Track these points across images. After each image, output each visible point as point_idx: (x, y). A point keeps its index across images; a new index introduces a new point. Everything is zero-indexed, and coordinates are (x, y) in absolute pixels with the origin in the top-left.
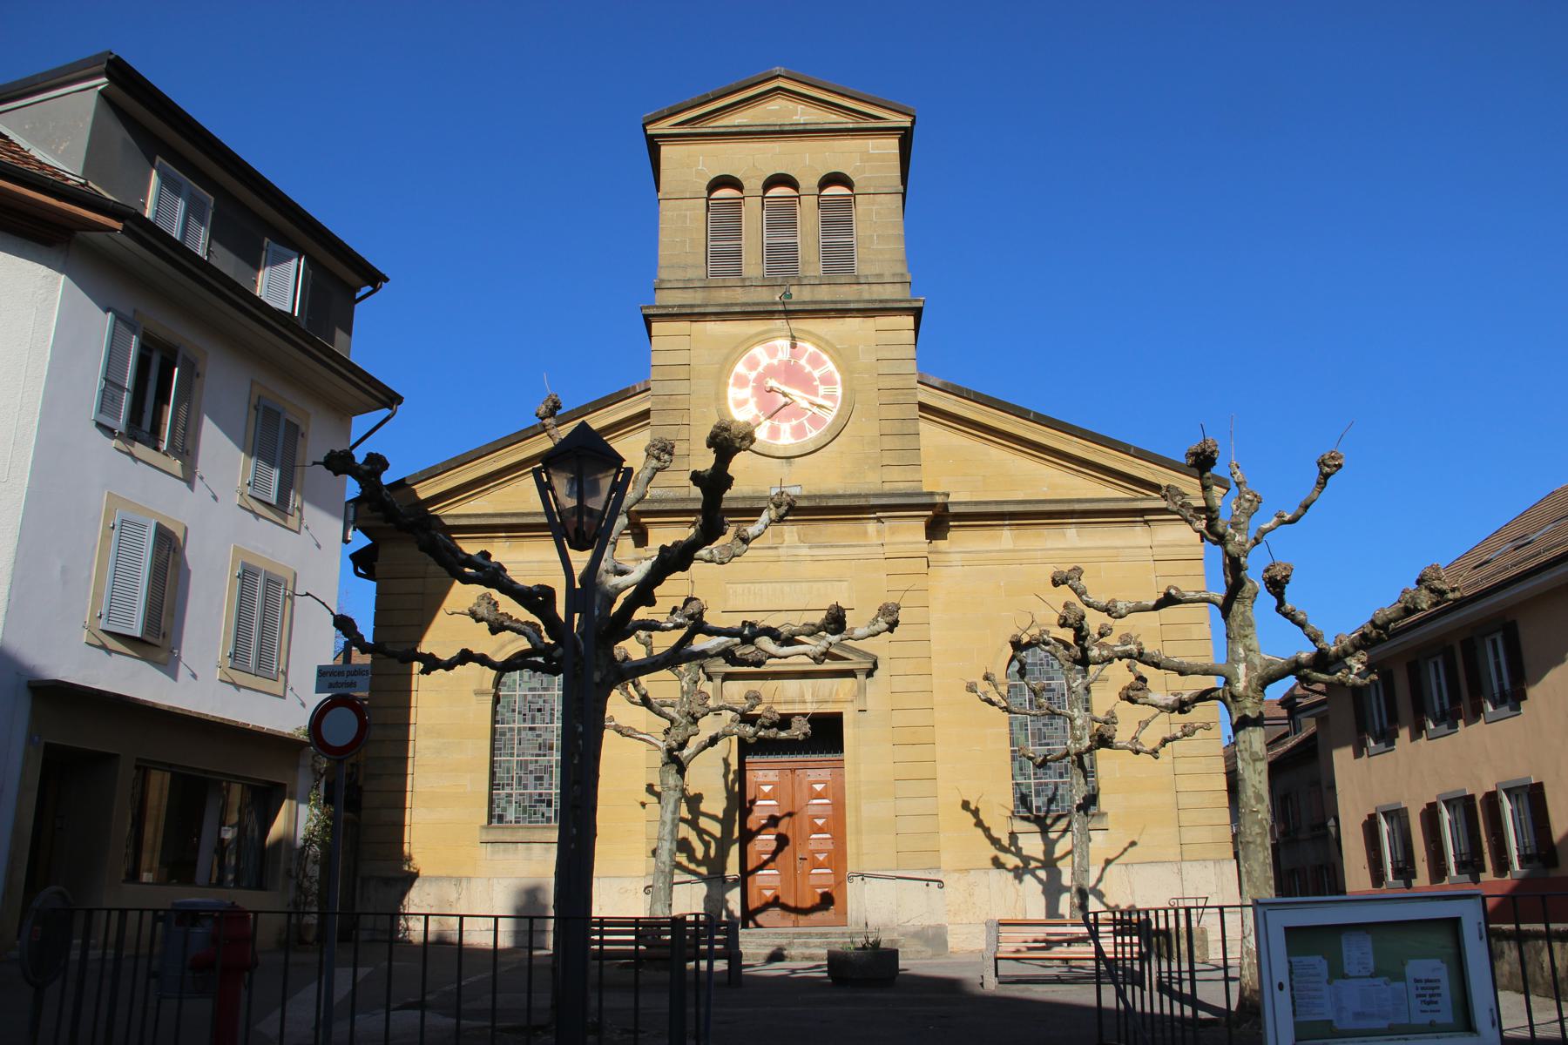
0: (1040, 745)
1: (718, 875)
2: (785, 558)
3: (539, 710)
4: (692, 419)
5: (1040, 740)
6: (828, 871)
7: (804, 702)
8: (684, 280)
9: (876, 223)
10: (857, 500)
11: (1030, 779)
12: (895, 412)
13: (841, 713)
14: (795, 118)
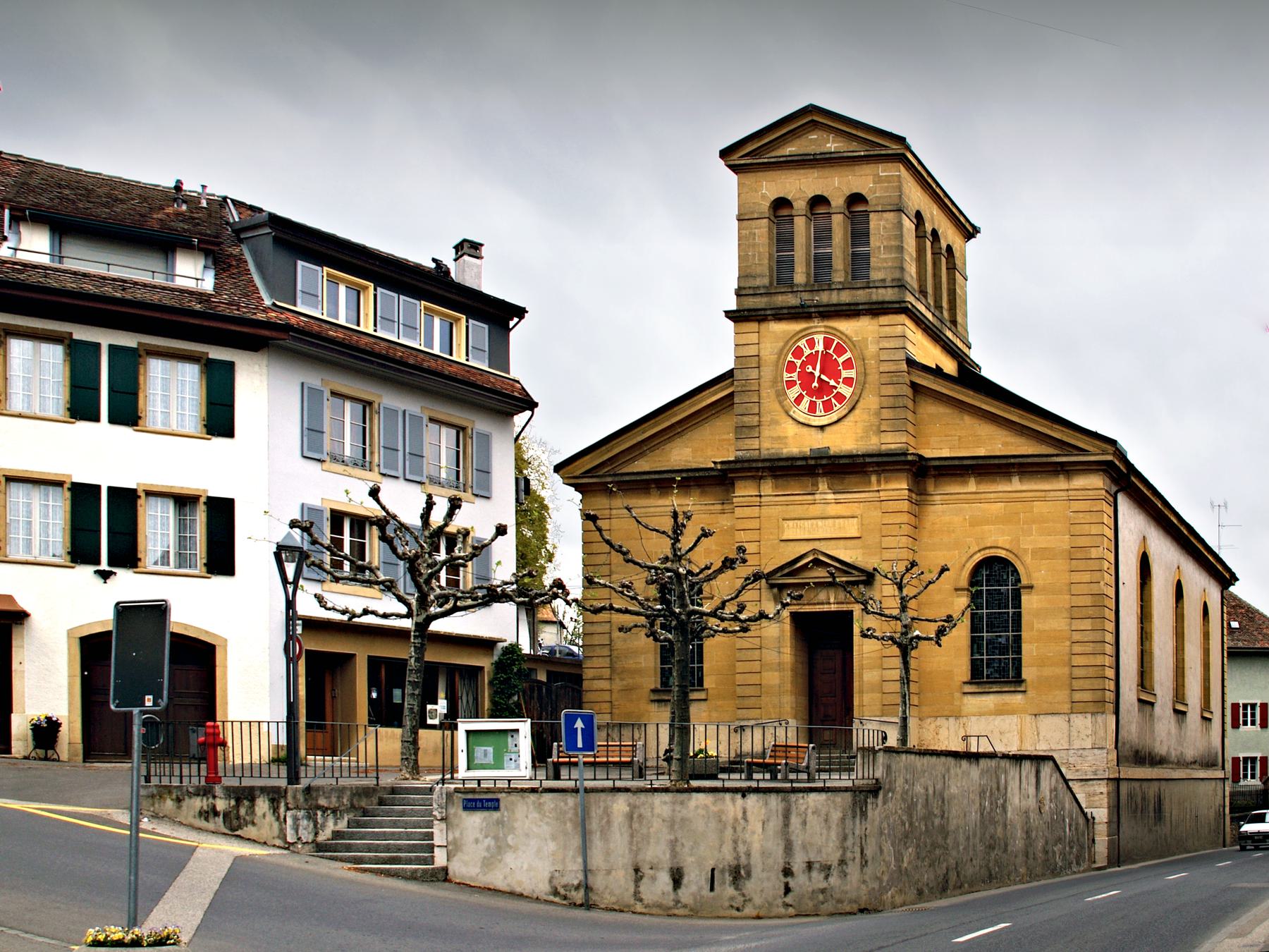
7: (829, 603)
8: (754, 288)
12: (890, 390)
13: (852, 611)
14: (828, 145)
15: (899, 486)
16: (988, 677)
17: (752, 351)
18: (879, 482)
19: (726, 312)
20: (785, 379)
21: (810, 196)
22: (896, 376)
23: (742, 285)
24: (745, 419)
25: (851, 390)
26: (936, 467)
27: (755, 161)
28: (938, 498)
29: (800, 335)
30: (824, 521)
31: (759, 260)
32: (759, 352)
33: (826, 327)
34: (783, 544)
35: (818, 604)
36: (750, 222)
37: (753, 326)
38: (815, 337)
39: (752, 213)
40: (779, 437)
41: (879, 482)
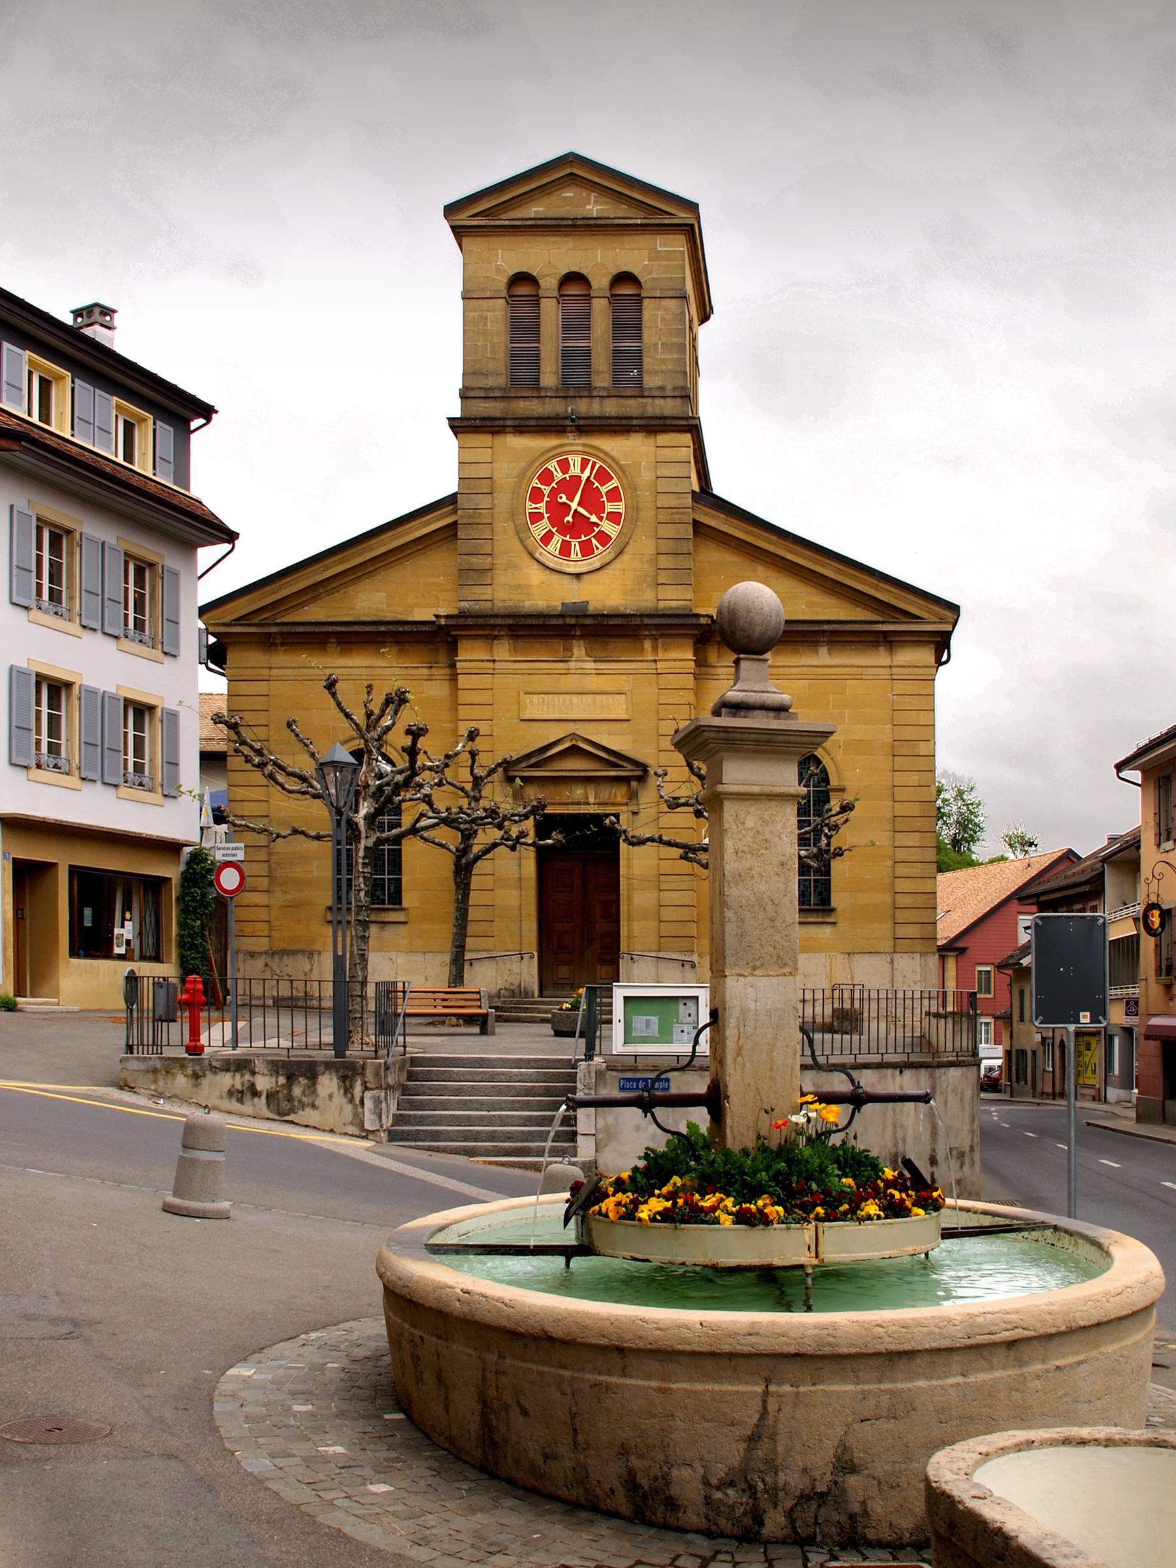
2: (574, 671)
7: (588, 804)
9: (661, 329)
12: (668, 531)
14: (588, 207)
15: (682, 656)
17: (483, 471)
22: (678, 513)
23: (468, 384)
24: (473, 560)
25: (618, 528)
27: (492, 223)
29: (551, 454)
31: (493, 352)
34: (524, 724)
35: (573, 804)
36: (480, 302)
37: (484, 439)
38: (570, 457)
39: (483, 290)
41: (655, 649)
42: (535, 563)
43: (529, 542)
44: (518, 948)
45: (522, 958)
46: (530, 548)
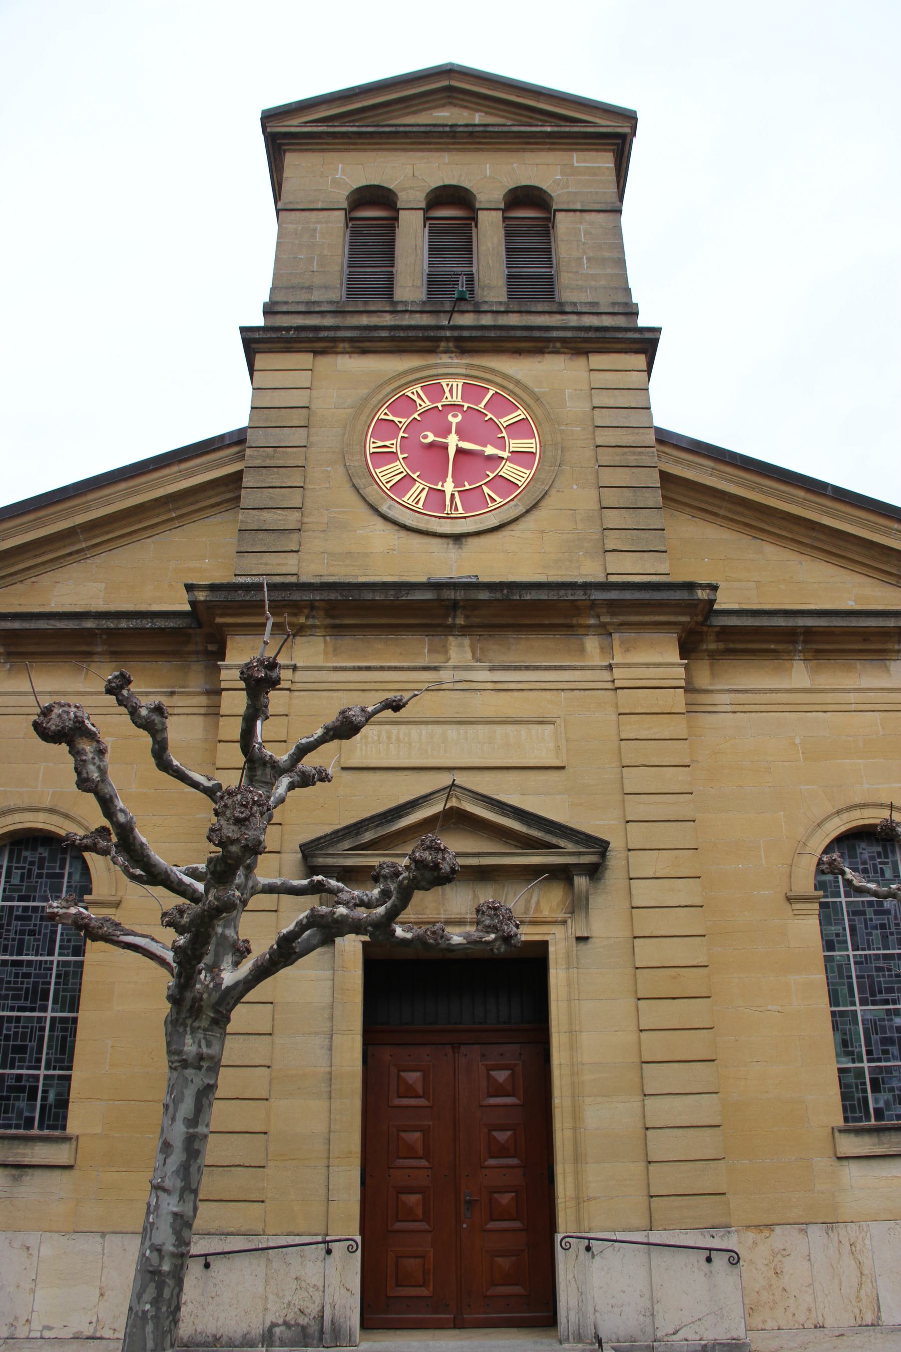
0: (874, 1003)
1: (319, 1239)
2: (450, 686)
3: (32, 933)
4: (307, 480)
5: (873, 994)
6: (517, 1224)
9: (584, 244)
10: (569, 592)
11: (862, 1061)
13: (546, 943)
16: (879, 1114)
18: (607, 650)
19: (243, 330)
20: (371, 448)
21: (434, 186)
22: (634, 454)
24: (266, 515)
26: (725, 633)
28: (726, 698)
30: (462, 728)
32: (310, 402)
33: (468, 366)
40: (349, 554)
41: (607, 650)
42: (379, 521)
43: (371, 492)
44: (321, 1229)
45: (329, 1252)
46: (371, 499)
